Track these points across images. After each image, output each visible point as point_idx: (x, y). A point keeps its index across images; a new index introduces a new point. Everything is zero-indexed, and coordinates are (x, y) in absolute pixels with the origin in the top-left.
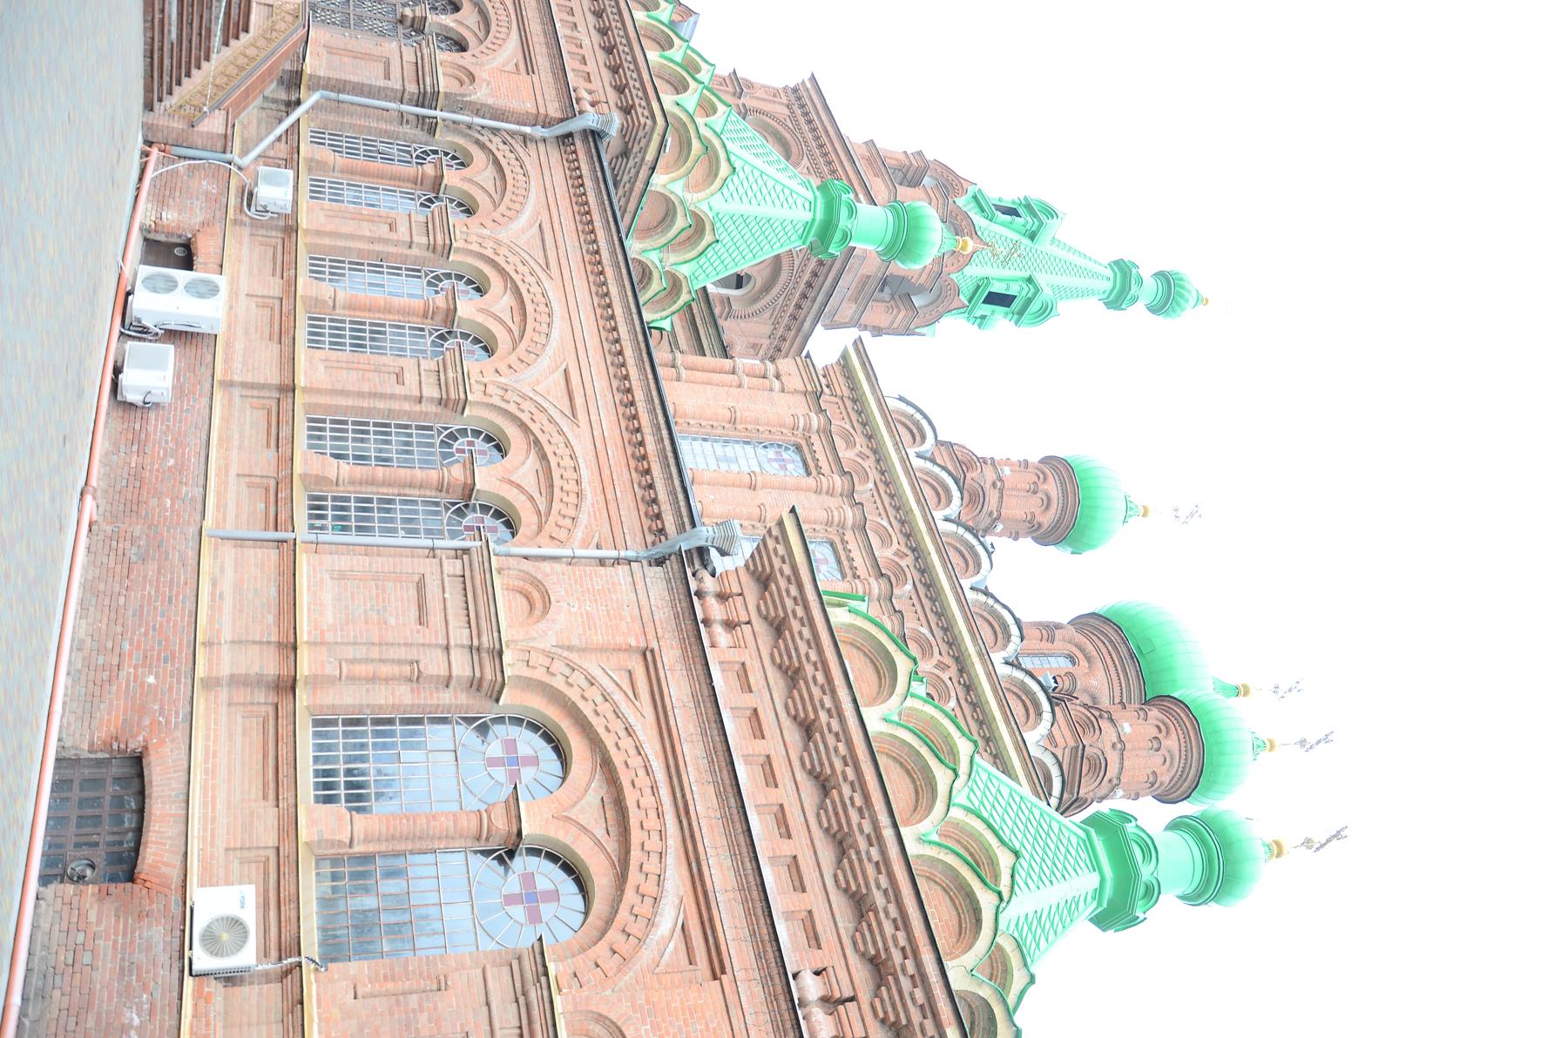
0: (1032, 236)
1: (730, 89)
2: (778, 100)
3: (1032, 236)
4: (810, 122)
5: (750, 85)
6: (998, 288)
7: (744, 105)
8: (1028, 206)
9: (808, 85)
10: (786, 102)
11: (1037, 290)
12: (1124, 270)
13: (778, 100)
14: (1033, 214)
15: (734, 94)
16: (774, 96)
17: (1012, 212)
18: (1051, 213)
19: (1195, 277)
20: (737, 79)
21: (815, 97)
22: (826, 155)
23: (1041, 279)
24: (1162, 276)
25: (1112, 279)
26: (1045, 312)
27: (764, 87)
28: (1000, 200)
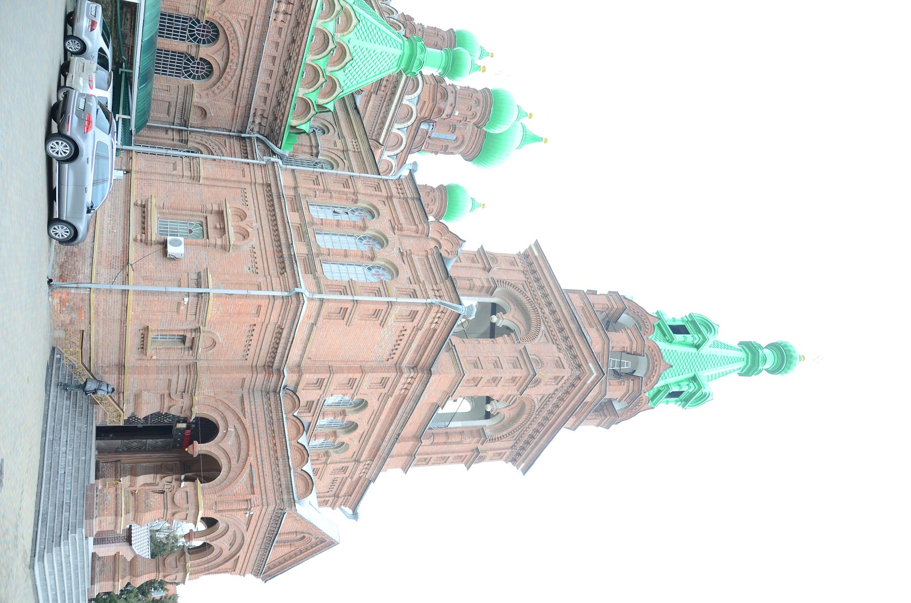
0: (697, 347)
1: (480, 265)
2: (517, 268)
3: (697, 347)
4: (542, 288)
5: (494, 258)
6: (675, 389)
7: (493, 279)
8: (693, 322)
9: (536, 254)
10: (522, 269)
11: (700, 387)
12: (751, 348)
13: (517, 268)
14: (699, 331)
15: (484, 269)
16: (512, 264)
17: (679, 330)
18: (710, 327)
19: (798, 346)
20: (485, 254)
21: (541, 262)
22: (558, 321)
23: (702, 376)
24: (774, 347)
25: (745, 360)
26: (704, 398)
27: (505, 256)
28: (674, 320)
